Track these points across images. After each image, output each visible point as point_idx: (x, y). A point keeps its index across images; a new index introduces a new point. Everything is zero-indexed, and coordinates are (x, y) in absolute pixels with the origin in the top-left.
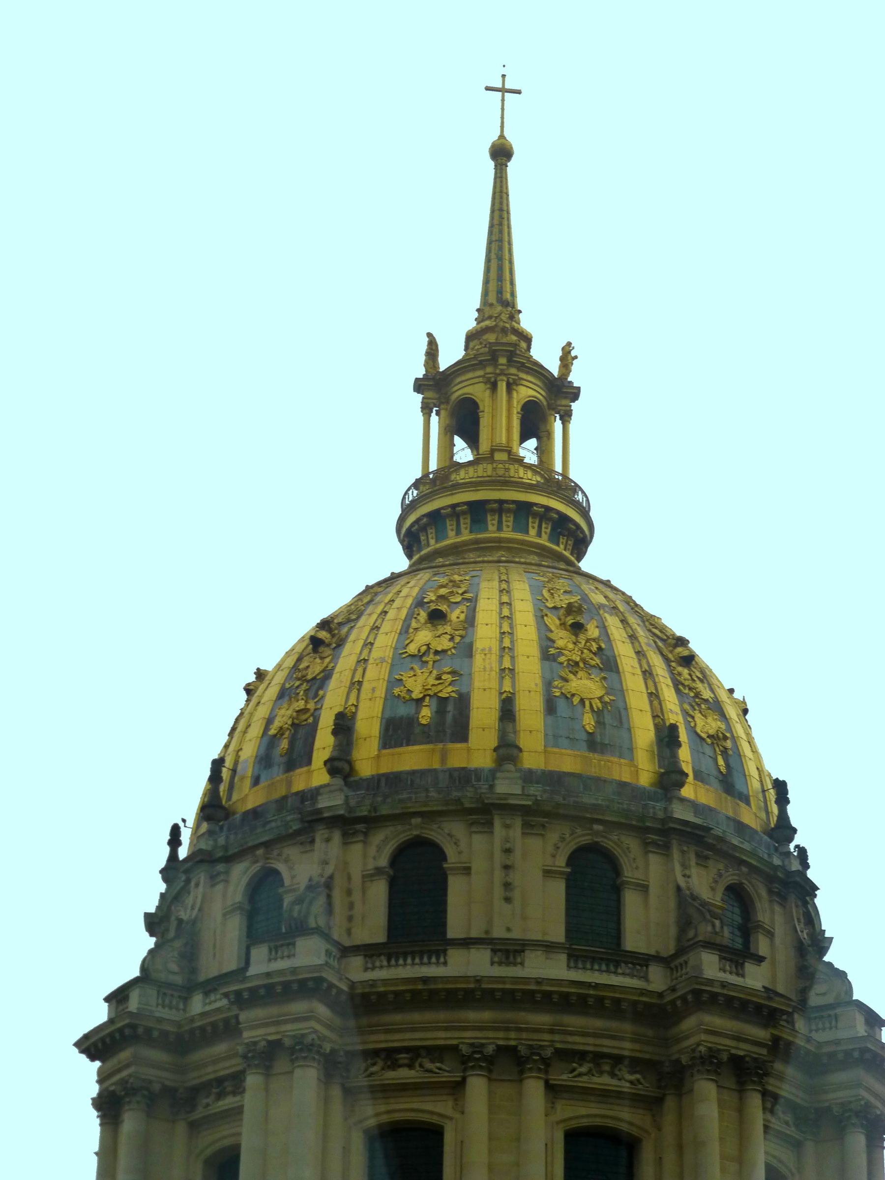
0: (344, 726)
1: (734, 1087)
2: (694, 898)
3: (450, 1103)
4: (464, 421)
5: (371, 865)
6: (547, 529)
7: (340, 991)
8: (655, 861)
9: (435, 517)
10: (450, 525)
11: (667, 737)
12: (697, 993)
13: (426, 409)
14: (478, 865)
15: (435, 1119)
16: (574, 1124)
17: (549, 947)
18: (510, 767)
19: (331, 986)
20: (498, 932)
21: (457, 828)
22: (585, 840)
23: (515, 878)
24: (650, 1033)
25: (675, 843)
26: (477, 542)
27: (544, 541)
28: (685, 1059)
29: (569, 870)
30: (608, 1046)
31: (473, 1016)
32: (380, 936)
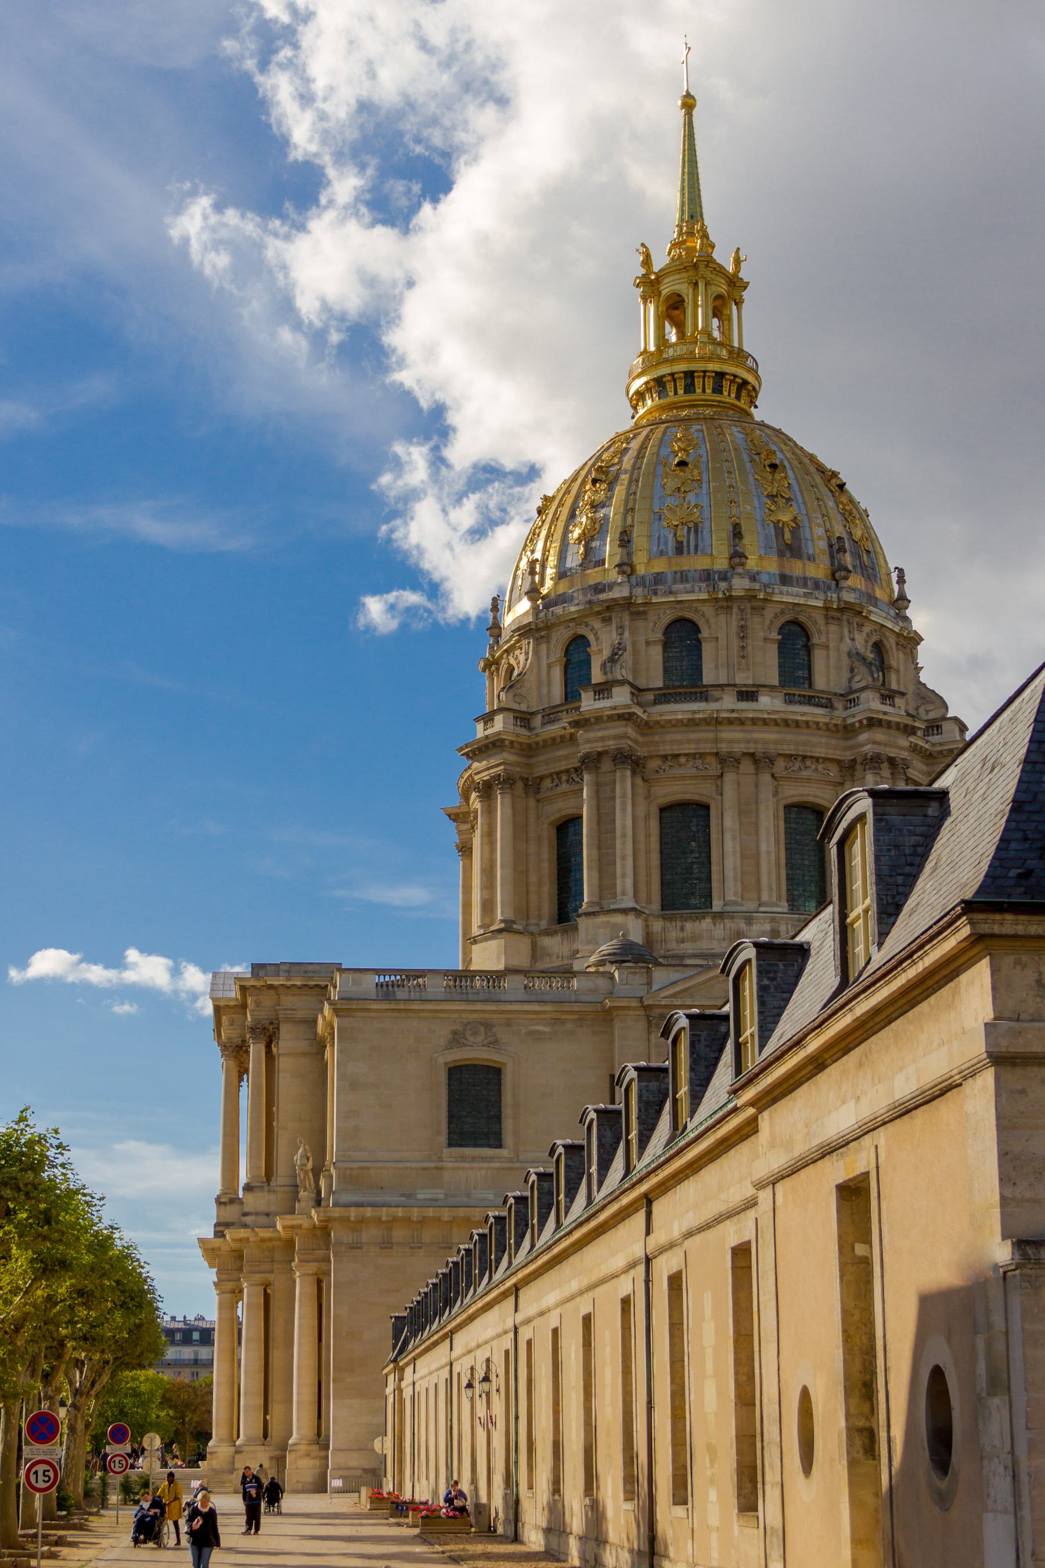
1: (889, 776)
3: (714, 788)
4: (673, 309)
6: (734, 388)
7: (642, 719)
8: (833, 628)
11: (836, 547)
12: (870, 719)
14: (722, 636)
15: (704, 799)
16: (789, 801)
17: (772, 688)
18: (740, 570)
19: (638, 717)
22: (788, 617)
27: (732, 399)
29: (780, 637)
32: (660, 684)
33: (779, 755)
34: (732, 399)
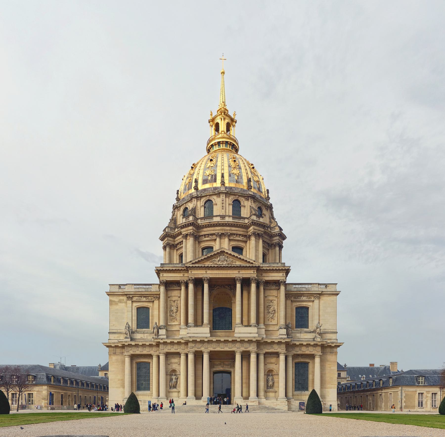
0: (196, 181)
2: (253, 208)
5: (201, 205)
6: (231, 147)
9: (212, 146)
10: (215, 147)
13: (212, 126)
17: (229, 216)
20: (221, 214)
21: (215, 197)
23: (224, 205)
24: (245, 230)
25: (249, 200)
26: (219, 149)
27: (230, 149)
28: (250, 234)
30: (239, 233)
31: (217, 228)
33: (230, 234)
34: (230, 149)
